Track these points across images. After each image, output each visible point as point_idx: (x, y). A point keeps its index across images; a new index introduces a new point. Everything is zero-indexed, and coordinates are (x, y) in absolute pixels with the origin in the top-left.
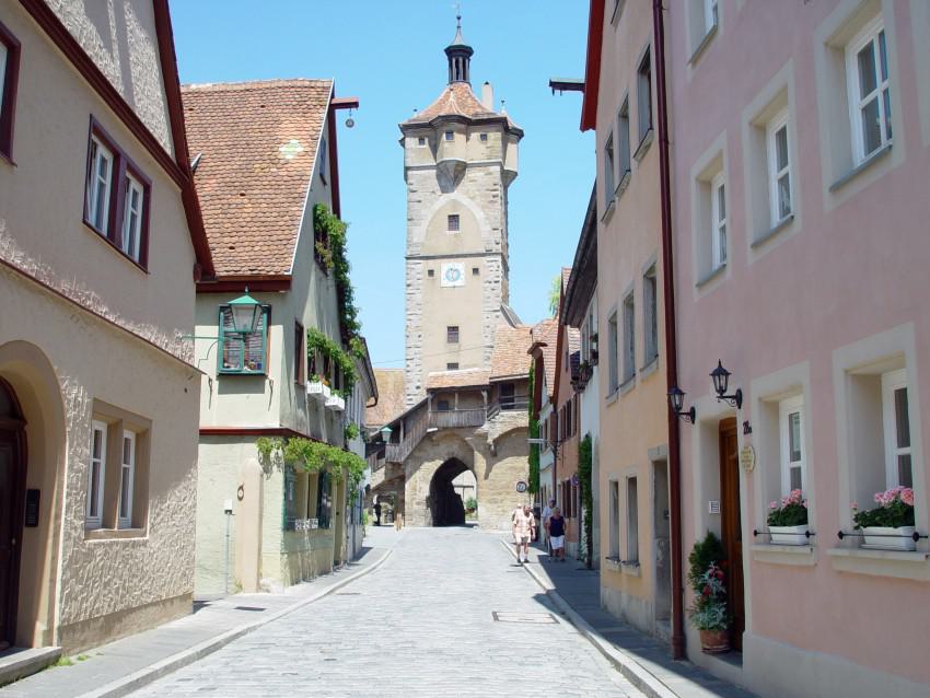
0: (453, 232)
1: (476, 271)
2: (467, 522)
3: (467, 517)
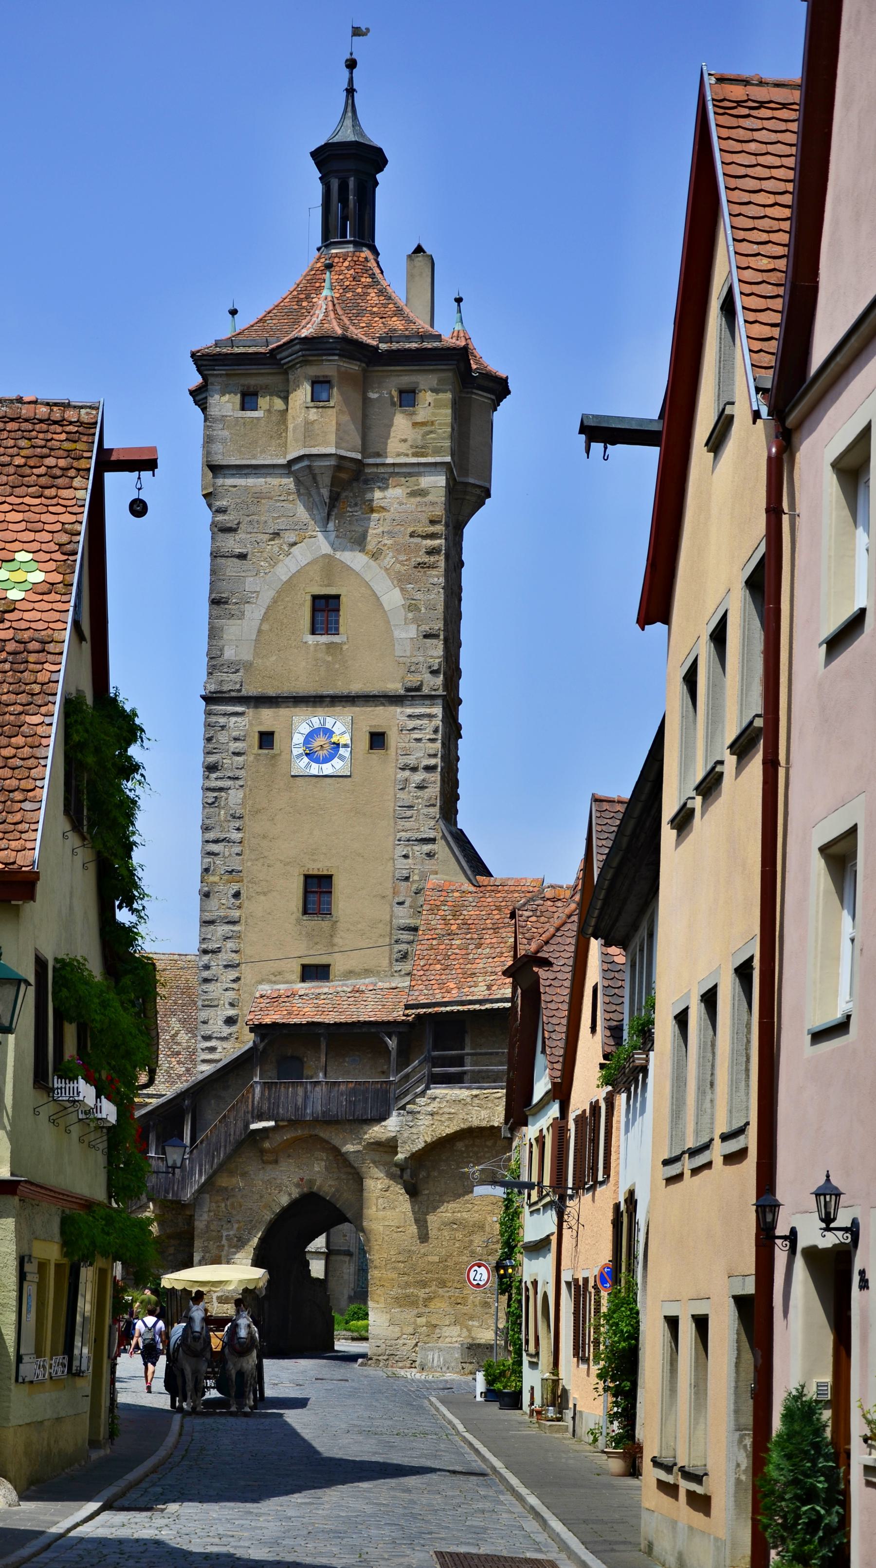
0: (324, 639)
1: (377, 740)
2: (342, 1345)
3: (339, 1332)
